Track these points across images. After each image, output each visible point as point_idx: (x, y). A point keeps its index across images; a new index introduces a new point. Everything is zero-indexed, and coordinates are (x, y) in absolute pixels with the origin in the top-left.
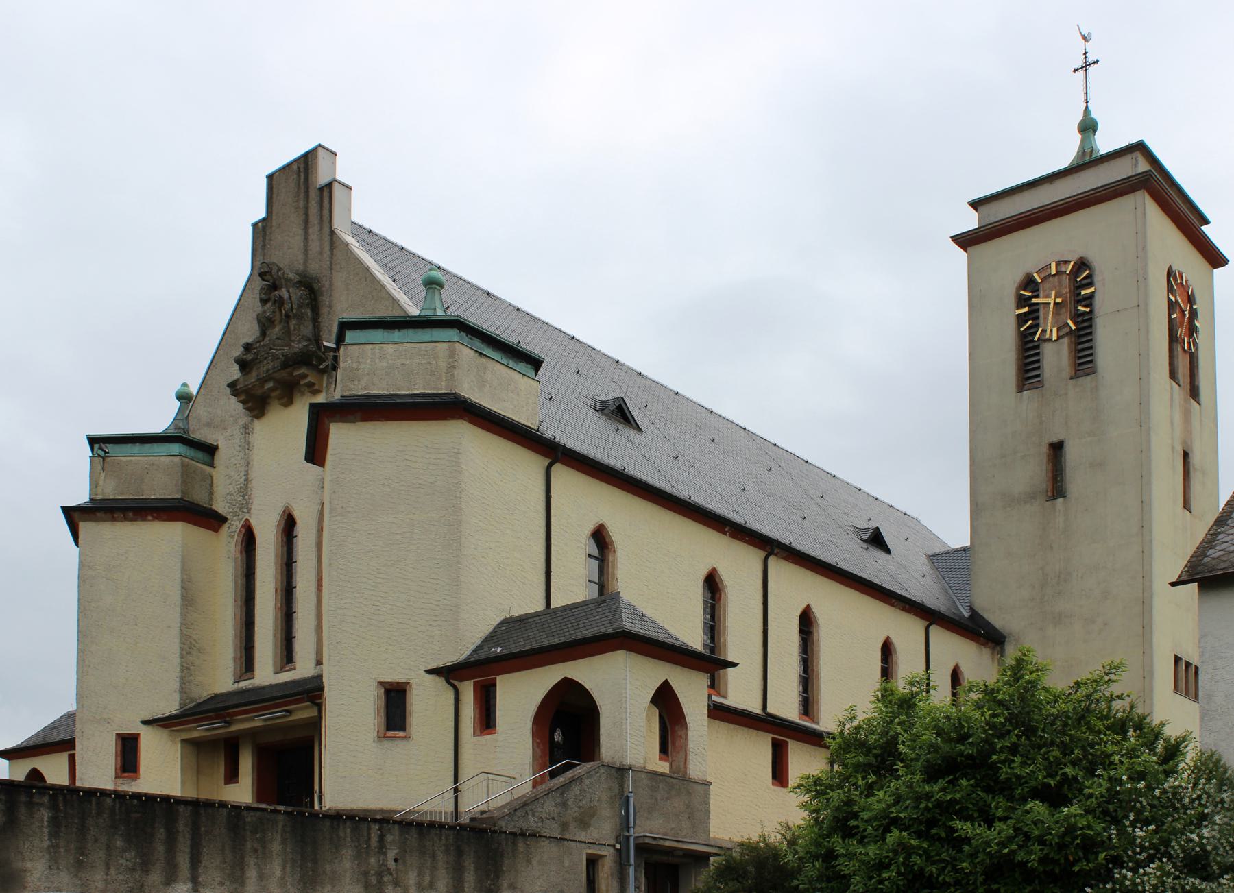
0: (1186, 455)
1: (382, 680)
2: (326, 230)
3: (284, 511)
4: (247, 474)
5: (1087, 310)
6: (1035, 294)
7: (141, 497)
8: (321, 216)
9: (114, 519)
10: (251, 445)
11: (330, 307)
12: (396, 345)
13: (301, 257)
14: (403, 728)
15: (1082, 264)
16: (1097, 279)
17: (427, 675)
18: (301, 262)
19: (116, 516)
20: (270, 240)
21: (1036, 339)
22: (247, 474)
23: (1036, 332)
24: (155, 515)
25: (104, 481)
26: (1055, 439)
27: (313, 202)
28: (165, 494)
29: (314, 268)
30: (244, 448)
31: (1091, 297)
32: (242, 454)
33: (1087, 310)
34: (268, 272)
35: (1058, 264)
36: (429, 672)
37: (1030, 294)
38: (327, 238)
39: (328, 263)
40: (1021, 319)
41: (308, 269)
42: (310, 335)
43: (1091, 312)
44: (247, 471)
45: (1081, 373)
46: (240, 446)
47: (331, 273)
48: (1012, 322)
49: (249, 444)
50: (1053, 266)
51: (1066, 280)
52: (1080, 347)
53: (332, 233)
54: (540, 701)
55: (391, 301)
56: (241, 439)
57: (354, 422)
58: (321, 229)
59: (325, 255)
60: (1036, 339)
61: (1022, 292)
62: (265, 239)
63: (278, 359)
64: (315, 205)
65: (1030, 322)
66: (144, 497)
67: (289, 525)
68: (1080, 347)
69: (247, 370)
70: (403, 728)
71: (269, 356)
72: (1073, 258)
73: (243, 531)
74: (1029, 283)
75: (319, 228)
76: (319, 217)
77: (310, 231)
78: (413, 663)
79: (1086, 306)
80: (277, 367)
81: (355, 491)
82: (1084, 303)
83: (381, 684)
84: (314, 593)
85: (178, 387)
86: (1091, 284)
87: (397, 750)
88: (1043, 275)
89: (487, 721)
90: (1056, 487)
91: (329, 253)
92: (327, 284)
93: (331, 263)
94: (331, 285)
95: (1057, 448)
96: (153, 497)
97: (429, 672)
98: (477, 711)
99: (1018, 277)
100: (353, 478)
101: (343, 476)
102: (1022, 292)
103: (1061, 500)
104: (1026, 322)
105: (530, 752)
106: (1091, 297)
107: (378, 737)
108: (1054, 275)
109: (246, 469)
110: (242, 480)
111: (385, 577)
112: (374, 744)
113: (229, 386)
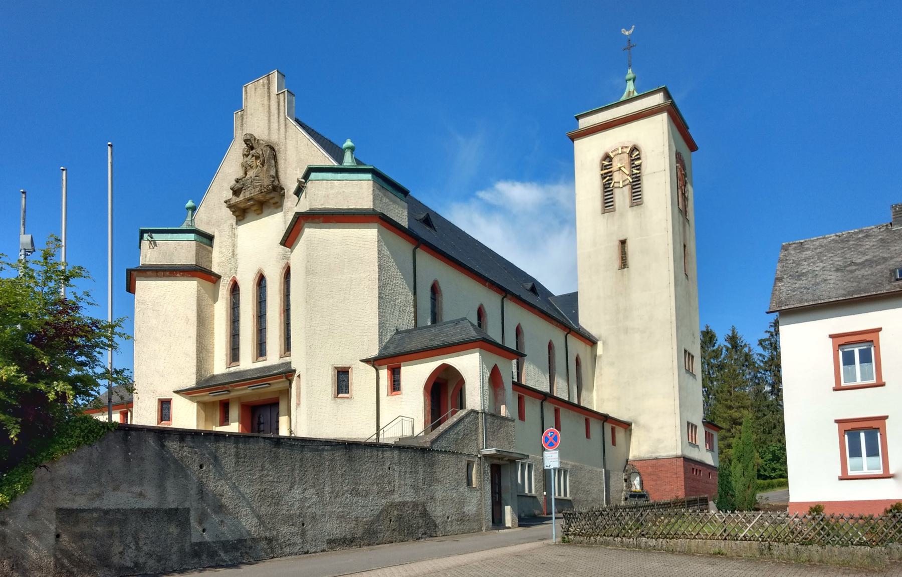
0: (685, 246)
1: (336, 366)
4: (233, 251)
5: (638, 172)
6: (610, 163)
7: (172, 264)
10: (236, 235)
11: (285, 160)
12: (339, 181)
13: (266, 132)
14: (347, 392)
15: (635, 148)
16: (643, 156)
17: (361, 363)
18: (267, 134)
19: (158, 274)
20: (246, 122)
21: (611, 186)
22: (233, 251)
23: (611, 183)
24: (181, 274)
26: (622, 238)
27: (273, 102)
28: (186, 262)
29: (274, 138)
30: (231, 237)
31: (640, 165)
32: (230, 240)
33: (638, 172)
35: (622, 148)
36: (362, 361)
37: (608, 163)
39: (284, 135)
40: (603, 177)
41: (271, 139)
42: (274, 175)
43: (640, 173)
44: (234, 250)
45: (635, 204)
46: (229, 236)
47: (286, 141)
48: (599, 178)
49: (234, 234)
50: (620, 149)
51: (626, 156)
52: (634, 191)
54: (428, 376)
57: (319, 223)
60: (611, 186)
61: (604, 162)
64: (274, 103)
65: (608, 178)
66: (174, 263)
67: (261, 281)
68: (634, 191)
70: (347, 392)
72: (630, 145)
73: (232, 283)
74: (607, 157)
78: (353, 356)
79: (638, 170)
81: (319, 261)
82: (636, 168)
83: (336, 368)
84: (278, 318)
86: (639, 159)
87: (344, 405)
88: (614, 153)
89: (395, 386)
90: (624, 263)
91: (284, 130)
92: (283, 148)
93: (285, 136)
94: (285, 147)
95: (623, 242)
96: (179, 264)
97: (362, 361)
98: (389, 382)
99: (601, 154)
100: (319, 254)
101: (313, 253)
102: (604, 162)
103: (626, 269)
104: (605, 177)
105: (423, 404)
106: (640, 165)
107: (334, 397)
108: (620, 154)
111: (336, 308)
112: (332, 402)
113: (226, 202)
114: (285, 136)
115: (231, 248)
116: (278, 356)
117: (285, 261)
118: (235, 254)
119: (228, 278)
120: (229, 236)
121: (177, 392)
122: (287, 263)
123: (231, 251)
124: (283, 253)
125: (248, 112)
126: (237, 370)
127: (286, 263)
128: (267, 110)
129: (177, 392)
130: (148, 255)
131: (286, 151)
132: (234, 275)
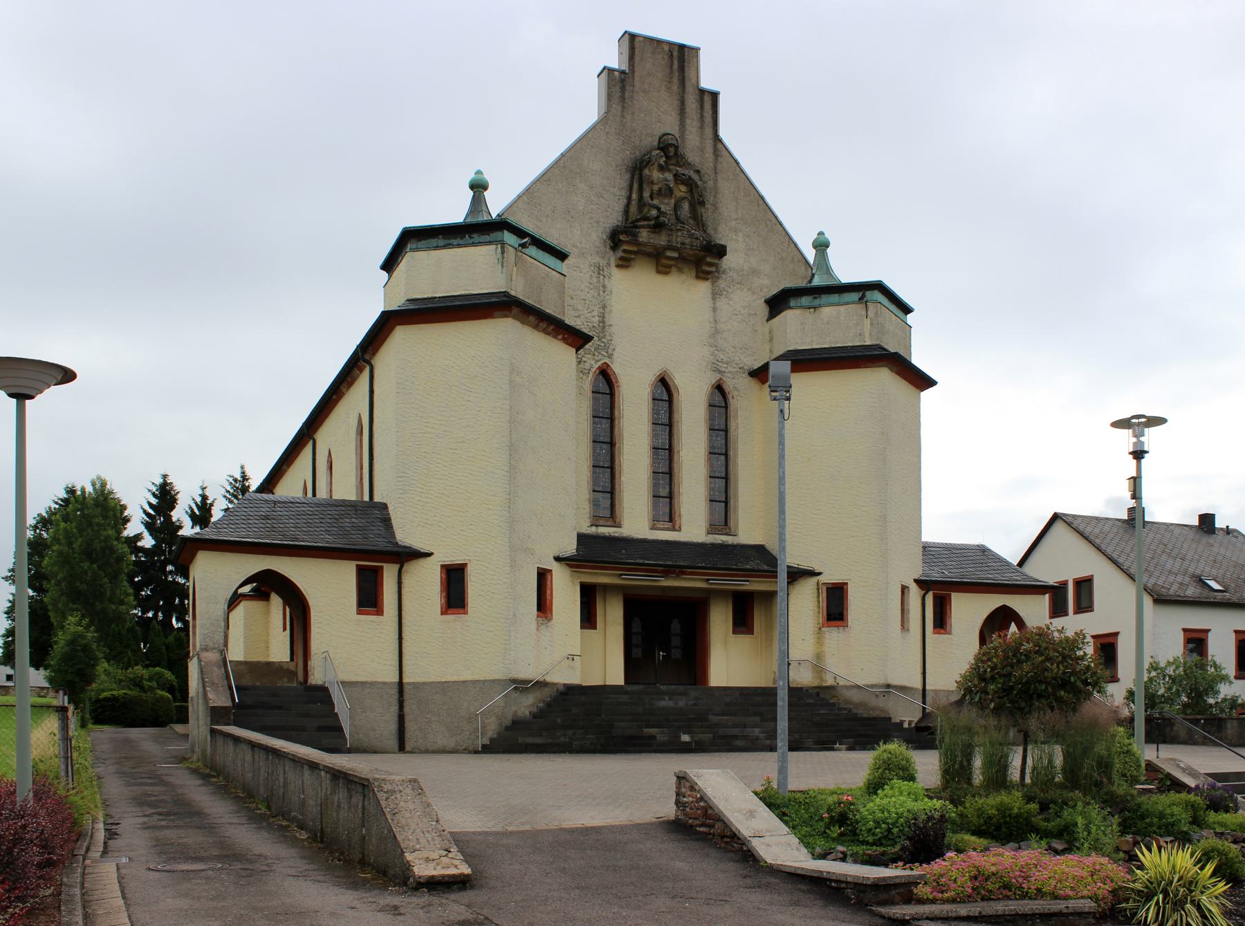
2: (708, 131)
3: (661, 374)
4: (602, 316)
8: (702, 116)
9: (536, 327)
10: (608, 289)
11: (715, 206)
22: (602, 316)
25: (516, 276)
34: (674, 145)
38: (709, 143)
46: (590, 283)
49: (604, 286)
53: (717, 139)
55: (787, 239)
56: (591, 276)
58: (702, 127)
59: (707, 155)
62: (624, 92)
63: (697, 238)
69: (657, 230)
71: (683, 230)
75: (699, 125)
76: (699, 116)
77: (688, 121)
80: (697, 246)
85: (471, 176)
109: (602, 311)
110: (597, 318)
114: (716, 168)
115: (596, 309)
116: (704, 531)
117: (718, 376)
118: (607, 324)
119: (593, 362)
120: (590, 283)
121: (558, 559)
122: (721, 379)
123: (595, 313)
124: (714, 361)
125: (637, 83)
126: (616, 535)
127: (718, 378)
128: (676, 103)
129: (557, 559)
130: (514, 278)
131: (716, 193)
132: (607, 360)
